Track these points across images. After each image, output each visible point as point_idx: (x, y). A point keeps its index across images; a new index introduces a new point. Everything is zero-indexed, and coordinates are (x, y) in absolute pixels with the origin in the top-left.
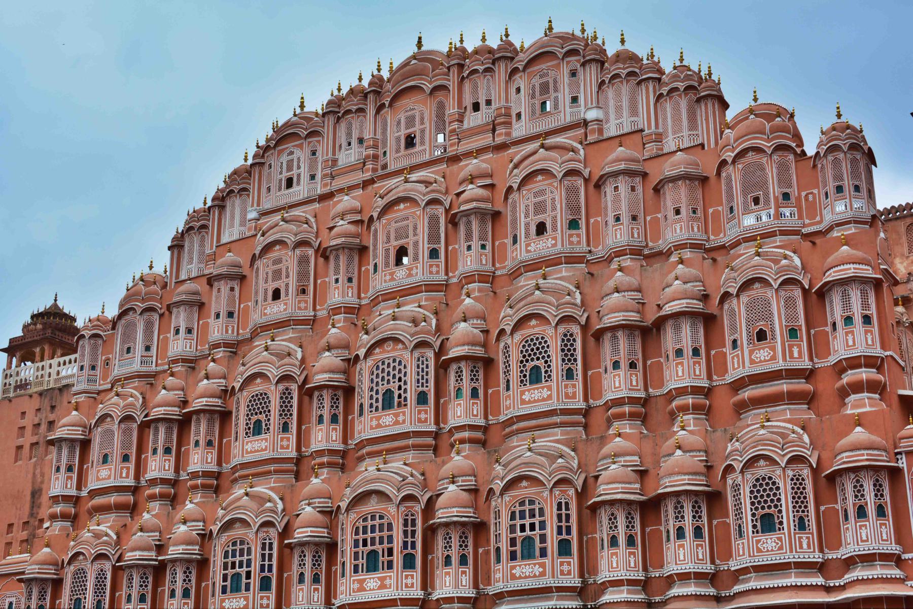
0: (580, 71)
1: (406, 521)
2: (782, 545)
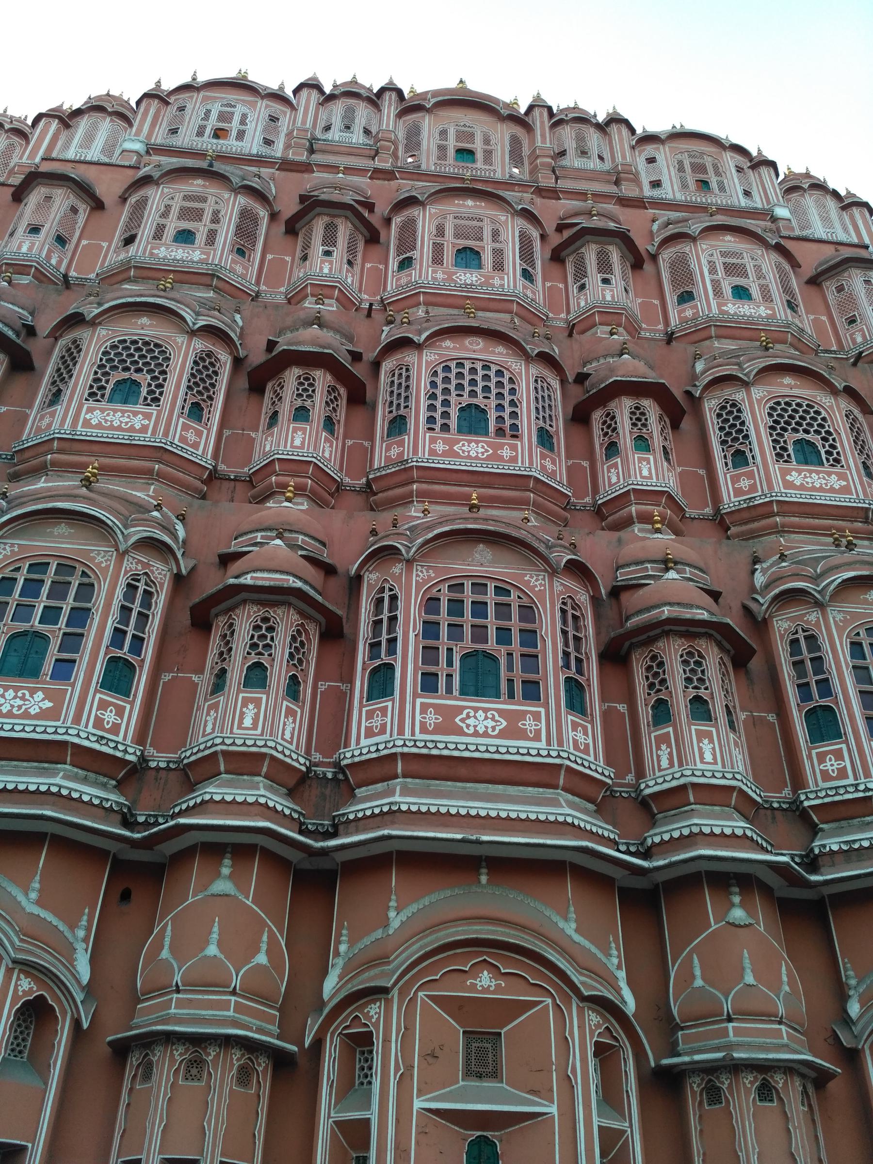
1: (563, 612)
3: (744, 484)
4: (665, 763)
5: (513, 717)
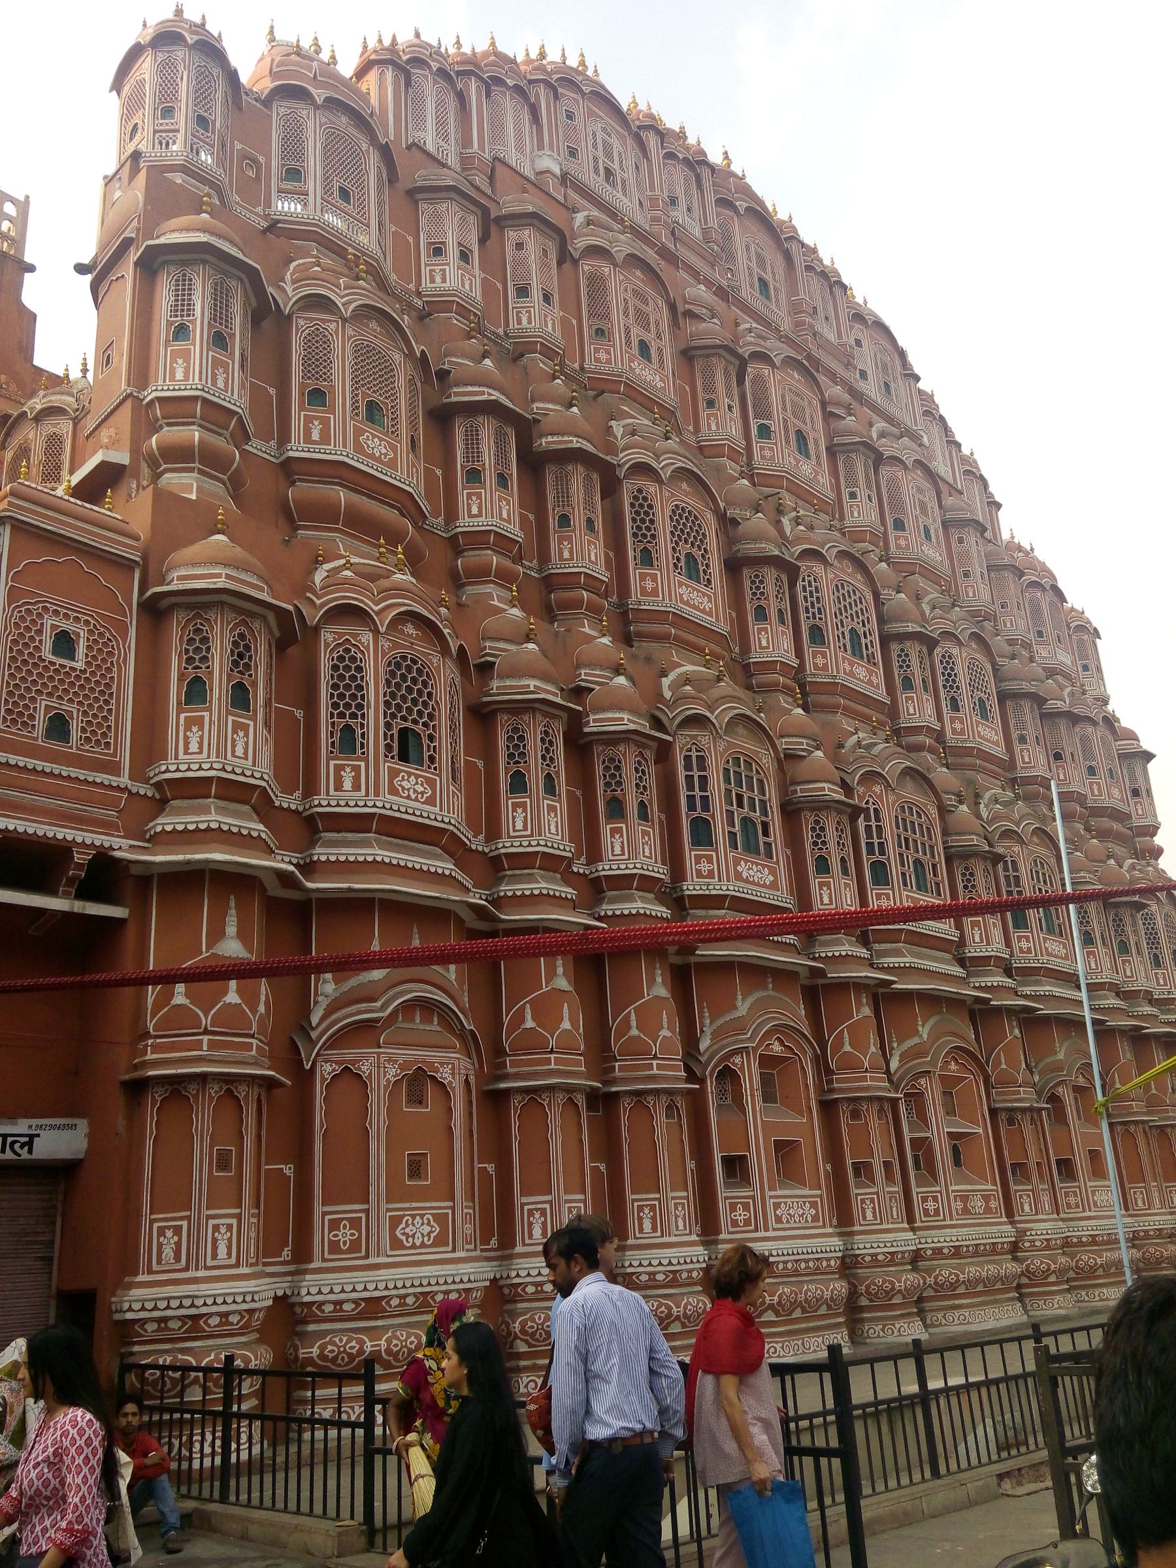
3: (958, 726)
4: (977, 939)
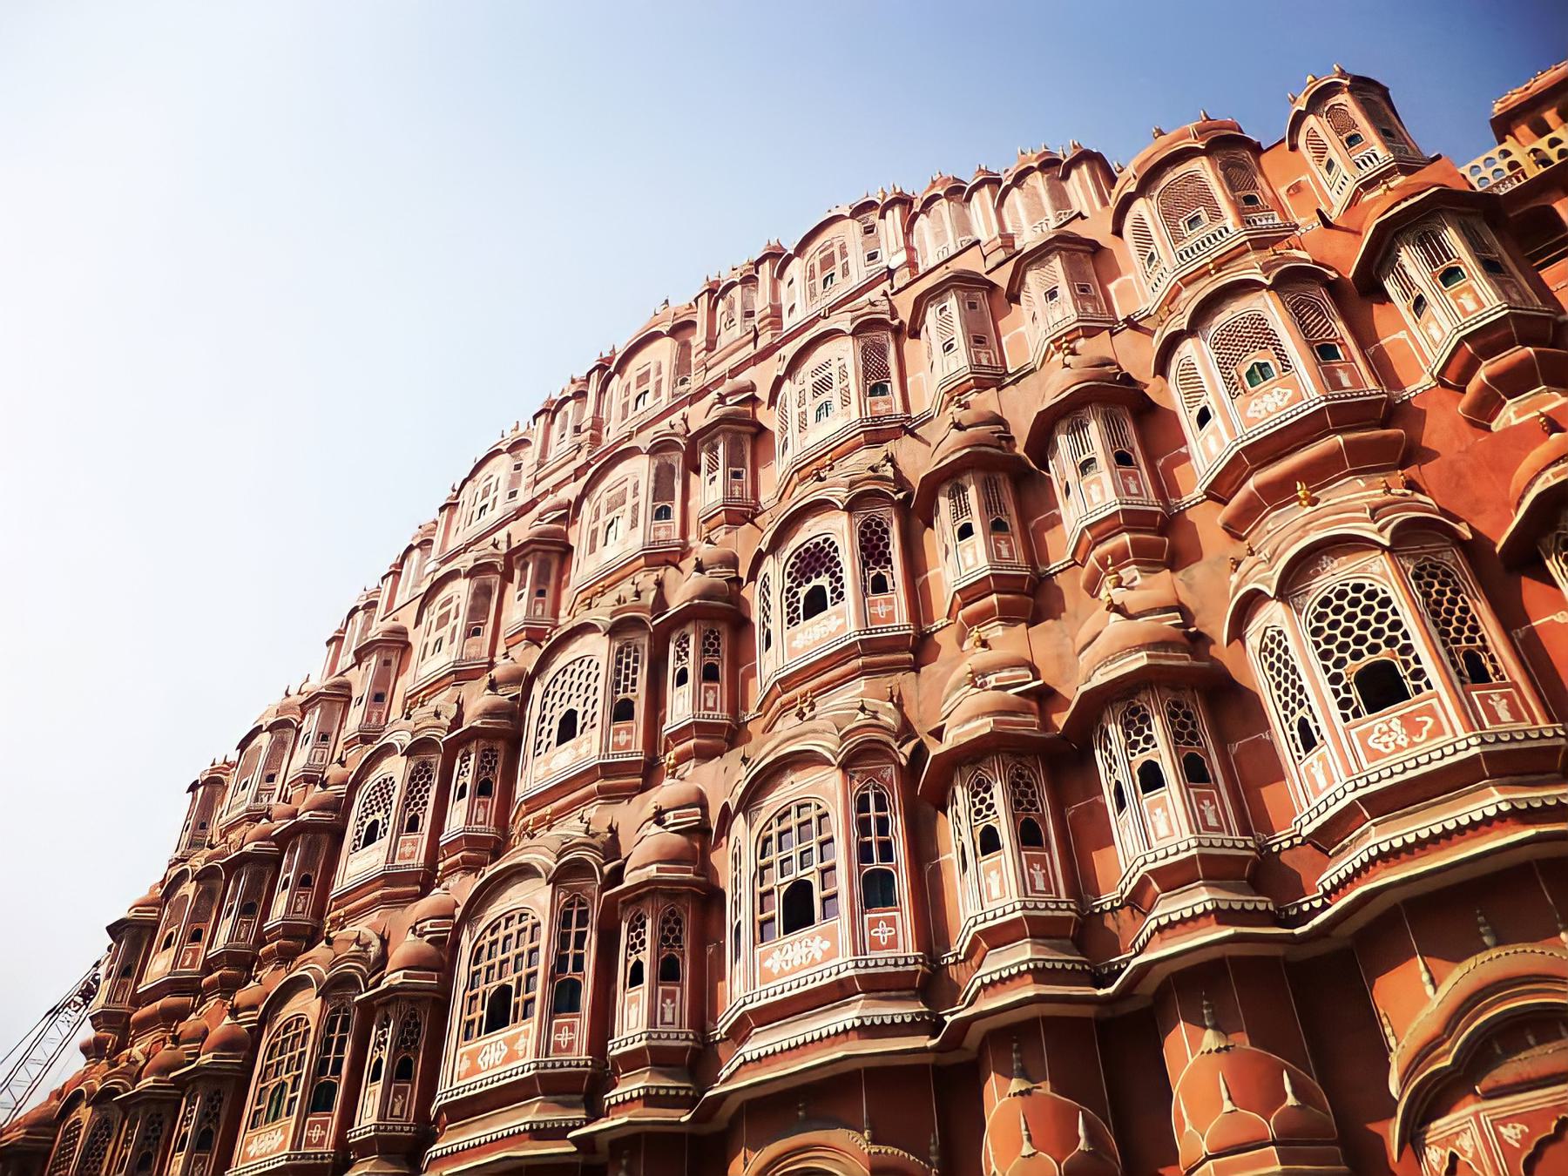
0: (880, 223)
2: (1438, 722)
5: (510, 1042)
